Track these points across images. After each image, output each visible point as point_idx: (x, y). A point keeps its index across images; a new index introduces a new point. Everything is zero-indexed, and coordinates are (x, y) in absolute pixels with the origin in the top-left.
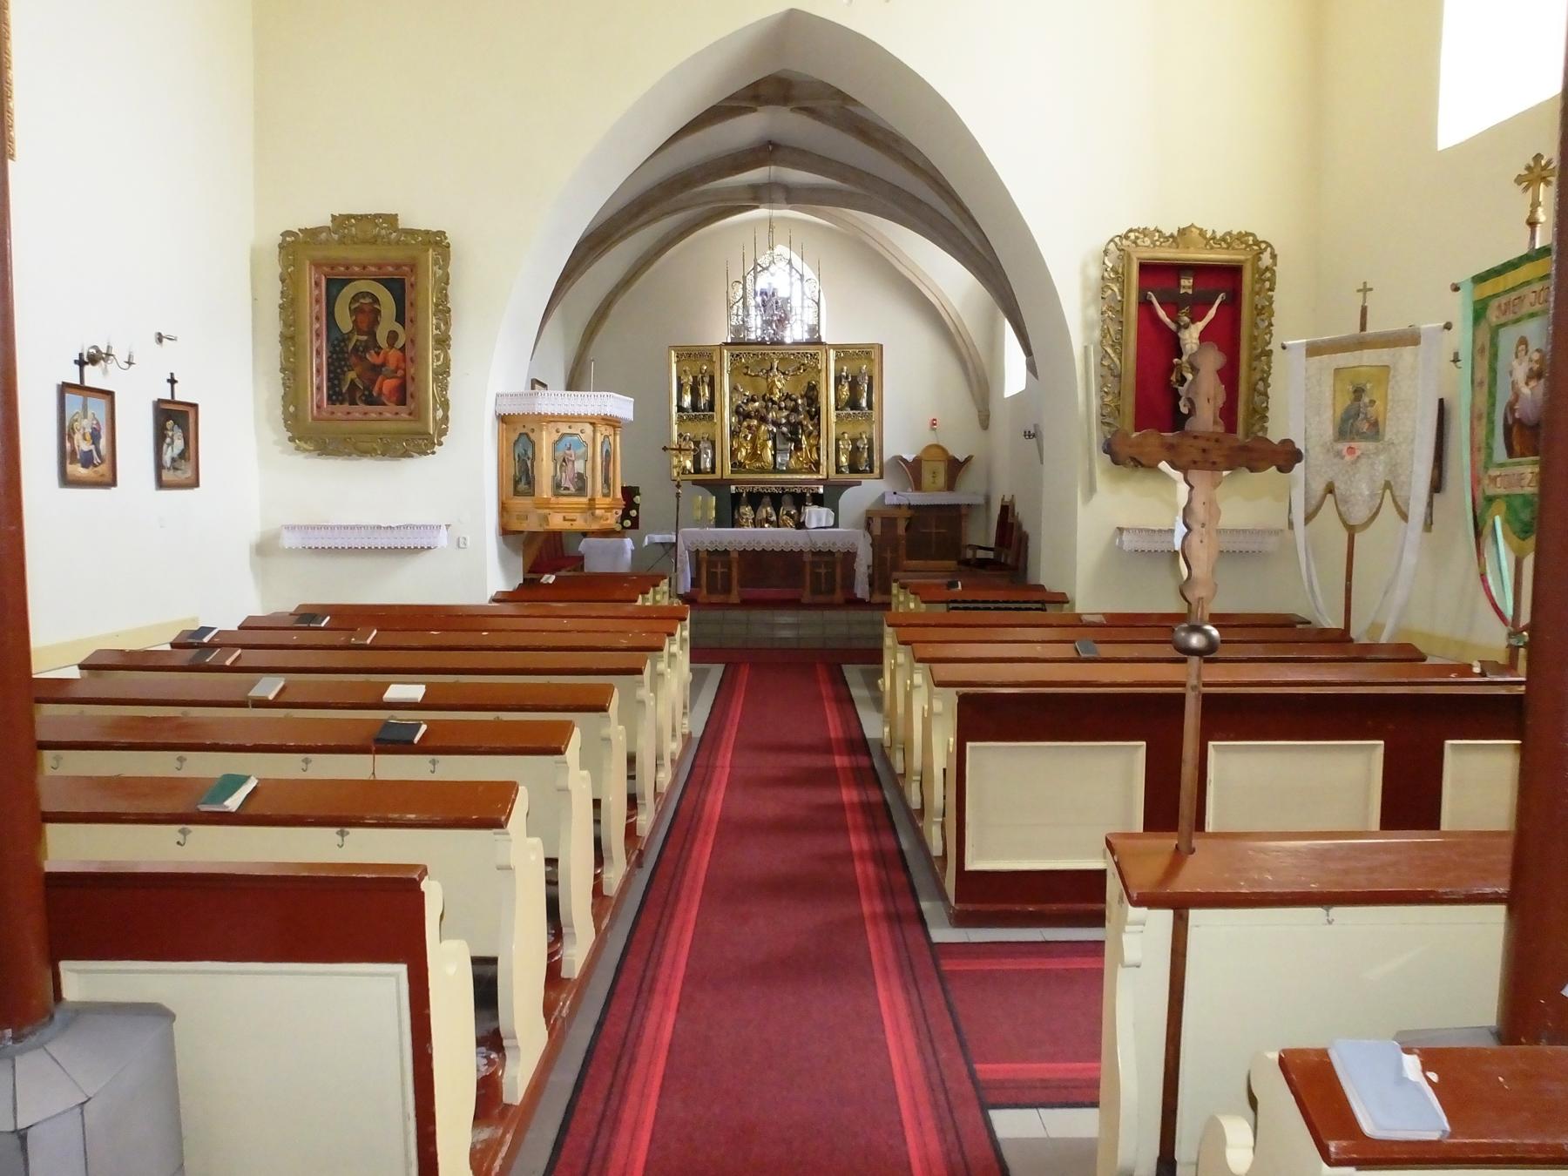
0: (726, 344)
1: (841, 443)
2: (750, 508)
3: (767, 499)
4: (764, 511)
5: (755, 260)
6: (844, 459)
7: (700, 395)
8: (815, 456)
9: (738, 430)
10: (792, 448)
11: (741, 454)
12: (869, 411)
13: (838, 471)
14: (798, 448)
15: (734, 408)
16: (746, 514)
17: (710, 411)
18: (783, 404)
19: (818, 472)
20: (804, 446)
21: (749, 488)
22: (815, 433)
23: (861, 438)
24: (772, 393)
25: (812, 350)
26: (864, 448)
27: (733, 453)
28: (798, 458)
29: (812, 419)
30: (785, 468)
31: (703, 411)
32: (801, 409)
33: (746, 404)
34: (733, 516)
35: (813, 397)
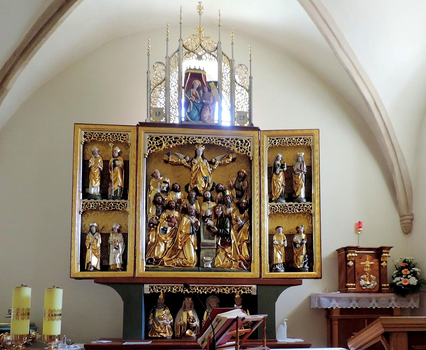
0: (142, 124)
1: (275, 238)
2: (168, 311)
3: (188, 301)
4: (185, 314)
5: (180, 40)
6: (279, 257)
7: (111, 181)
8: (245, 252)
9: (155, 221)
10: (219, 243)
11: (159, 249)
12: (309, 203)
13: (273, 268)
14: (226, 242)
15: (152, 198)
16: (162, 319)
17: (122, 198)
18: (209, 195)
19: (250, 270)
20: (233, 242)
21: (167, 288)
22: (246, 227)
23: (299, 232)
24: (196, 182)
25: (246, 135)
26: (302, 244)
27: (149, 248)
28: (226, 255)
29: (242, 212)
30: (210, 266)
31: (114, 198)
32: (229, 201)
33: (166, 193)
34: (147, 321)
35: (244, 188)
